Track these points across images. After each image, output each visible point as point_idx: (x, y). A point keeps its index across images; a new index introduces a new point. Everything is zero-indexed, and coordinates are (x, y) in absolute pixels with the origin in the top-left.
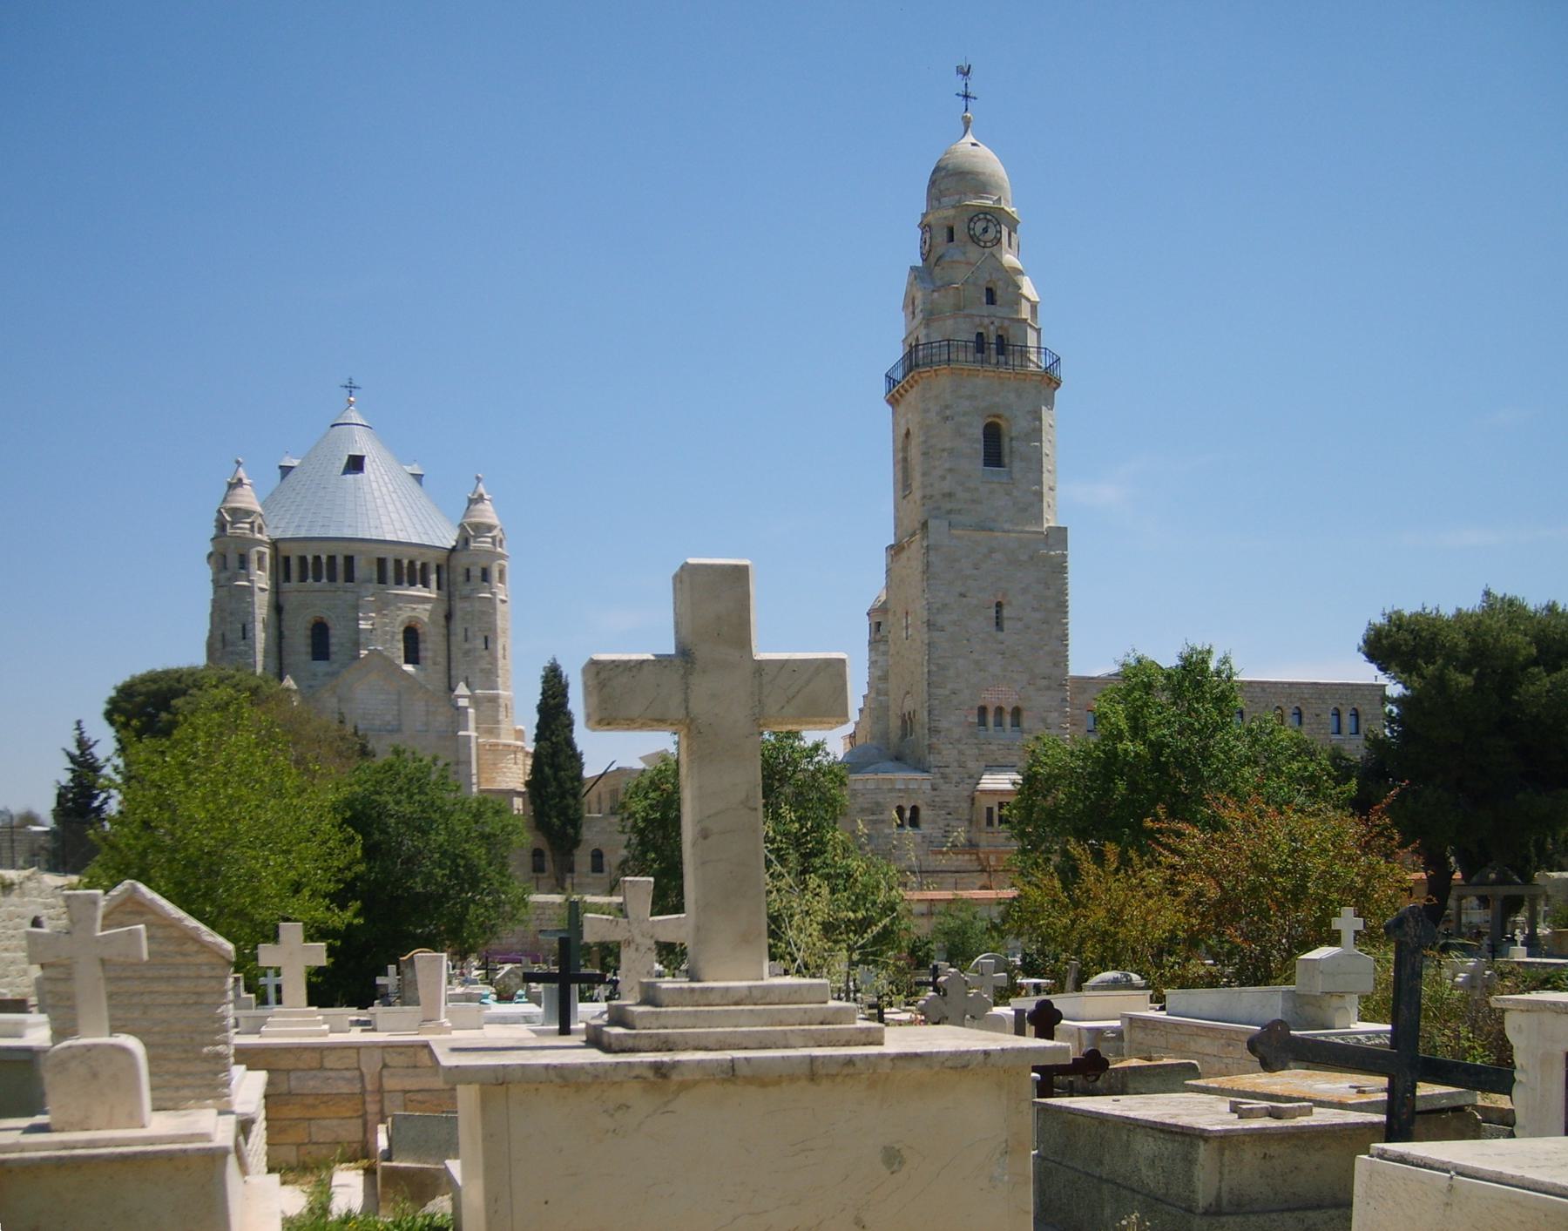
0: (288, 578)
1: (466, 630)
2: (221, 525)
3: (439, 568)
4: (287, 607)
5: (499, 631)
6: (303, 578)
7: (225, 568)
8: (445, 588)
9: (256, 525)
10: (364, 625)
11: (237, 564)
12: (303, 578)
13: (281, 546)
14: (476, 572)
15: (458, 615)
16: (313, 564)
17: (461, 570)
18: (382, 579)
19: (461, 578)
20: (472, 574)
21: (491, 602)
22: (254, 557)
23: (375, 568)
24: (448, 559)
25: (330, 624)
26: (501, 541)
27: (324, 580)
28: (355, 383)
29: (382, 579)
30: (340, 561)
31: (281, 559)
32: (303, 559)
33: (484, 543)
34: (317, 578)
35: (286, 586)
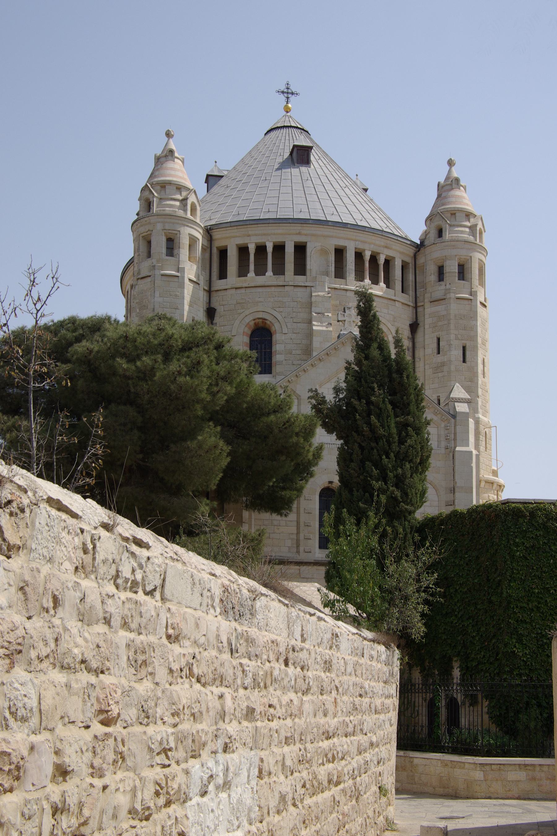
0: (223, 275)
1: (439, 340)
2: (147, 204)
3: (404, 267)
4: (220, 310)
5: (479, 340)
6: (243, 271)
7: (149, 255)
8: (411, 292)
9: (189, 202)
10: (317, 327)
11: (164, 250)
12: (243, 271)
13: (216, 235)
14: (452, 268)
15: (427, 322)
16: (256, 254)
17: (432, 269)
18: (340, 273)
19: (432, 277)
20: (447, 269)
21: (471, 301)
22: (185, 242)
23: (332, 258)
24: (415, 257)
25: (276, 327)
26: (481, 233)
27: (269, 273)
28: (293, 89)
29: (340, 273)
30: (290, 250)
31: (215, 251)
32: (243, 251)
33: (463, 233)
34: (260, 271)
35: (219, 284)
